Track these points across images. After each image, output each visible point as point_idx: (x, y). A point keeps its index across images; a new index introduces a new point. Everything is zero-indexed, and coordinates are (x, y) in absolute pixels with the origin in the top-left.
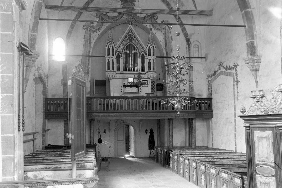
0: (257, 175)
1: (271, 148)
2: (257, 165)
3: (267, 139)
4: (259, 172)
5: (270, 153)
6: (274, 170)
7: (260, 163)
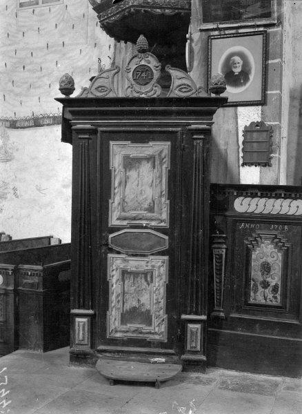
0: (110, 255)
3: (154, 162)
4: (119, 246)
5: (161, 196)
6: (167, 238)
7: (125, 223)
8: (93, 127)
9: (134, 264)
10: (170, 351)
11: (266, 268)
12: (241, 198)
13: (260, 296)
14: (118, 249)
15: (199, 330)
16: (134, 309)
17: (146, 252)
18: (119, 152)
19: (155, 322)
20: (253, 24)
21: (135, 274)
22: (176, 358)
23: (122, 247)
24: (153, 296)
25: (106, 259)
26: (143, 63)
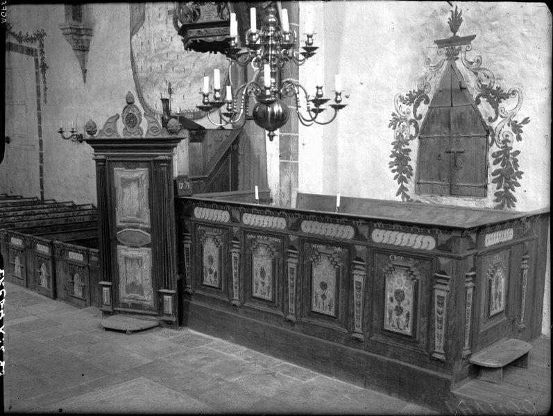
0: (118, 246)
1: (145, 199)
2: (121, 228)
6: (149, 235)
7: (124, 224)
9: (133, 253)
11: (211, 259)
12: (198, 208)
15: (171, 301)
16: (133, 284)
17: (137, 245)
18: (120, 173)
19: (146, 293)
21: (132, 260)
26: (131, 112)
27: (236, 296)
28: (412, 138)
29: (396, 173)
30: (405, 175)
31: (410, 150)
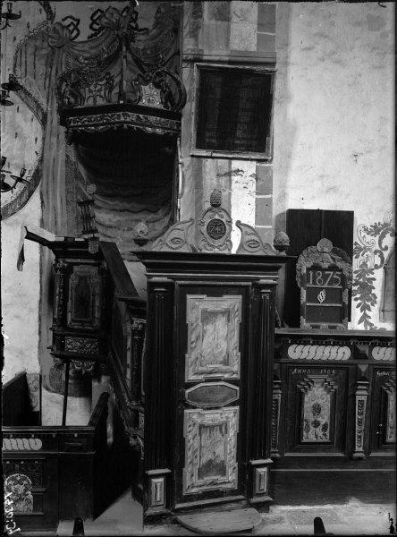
0: (187, 411)
6: (238, 388)
7: (201, 377)
8: (170, 280)
9: (210, 417)
10: (241, 497)
13: (311, 435)
14: (194, 404)
16: (210, 462)
19: (230, 471)
20: (248, 157)
21: (211, 428)
22: (244, 502)
23: (198, 401)
24: (226, 448)
25: (182, 416)
26: (217, 217)
27: (359, 447)
28: (377, 267)
29: (359, 301)
30: (369, 303)
31: (374, 279)
